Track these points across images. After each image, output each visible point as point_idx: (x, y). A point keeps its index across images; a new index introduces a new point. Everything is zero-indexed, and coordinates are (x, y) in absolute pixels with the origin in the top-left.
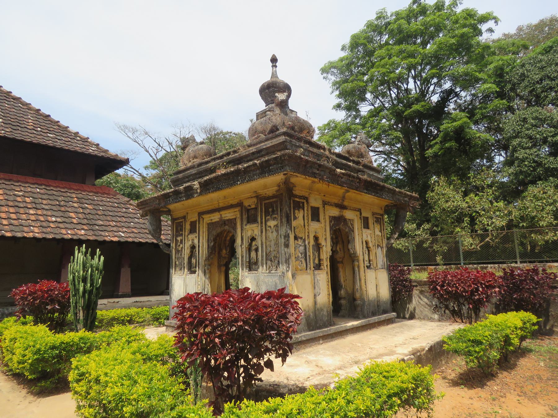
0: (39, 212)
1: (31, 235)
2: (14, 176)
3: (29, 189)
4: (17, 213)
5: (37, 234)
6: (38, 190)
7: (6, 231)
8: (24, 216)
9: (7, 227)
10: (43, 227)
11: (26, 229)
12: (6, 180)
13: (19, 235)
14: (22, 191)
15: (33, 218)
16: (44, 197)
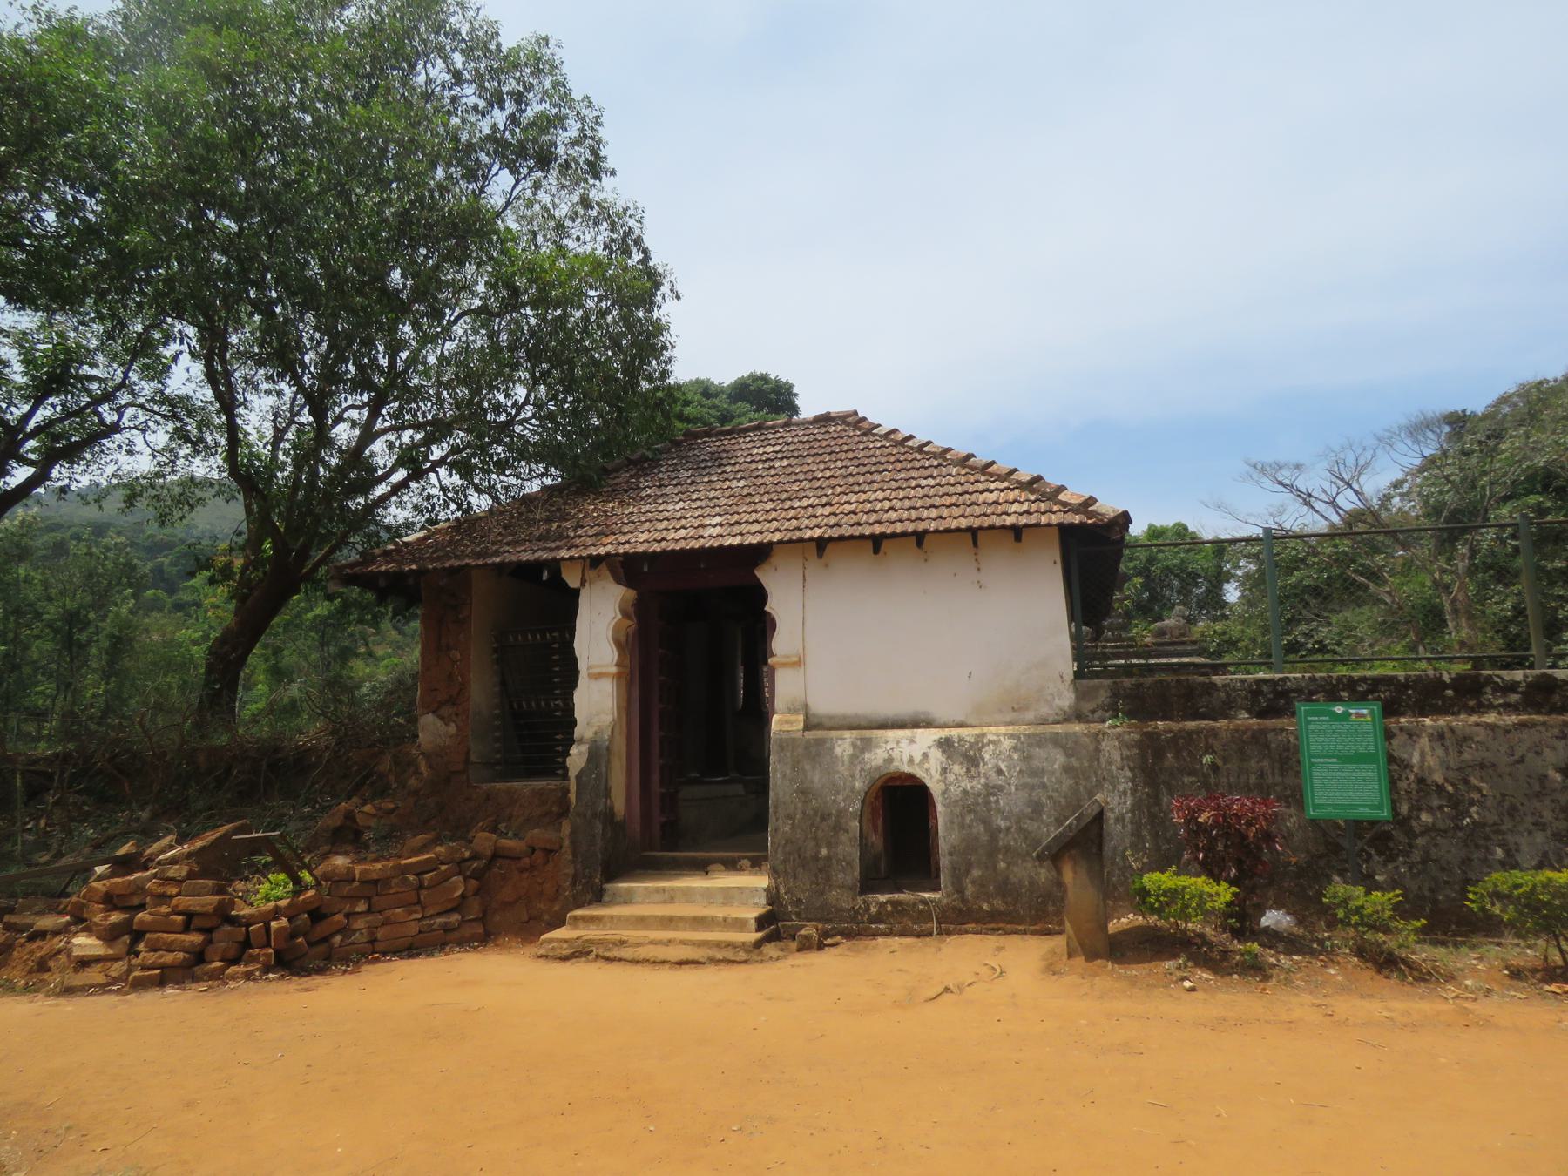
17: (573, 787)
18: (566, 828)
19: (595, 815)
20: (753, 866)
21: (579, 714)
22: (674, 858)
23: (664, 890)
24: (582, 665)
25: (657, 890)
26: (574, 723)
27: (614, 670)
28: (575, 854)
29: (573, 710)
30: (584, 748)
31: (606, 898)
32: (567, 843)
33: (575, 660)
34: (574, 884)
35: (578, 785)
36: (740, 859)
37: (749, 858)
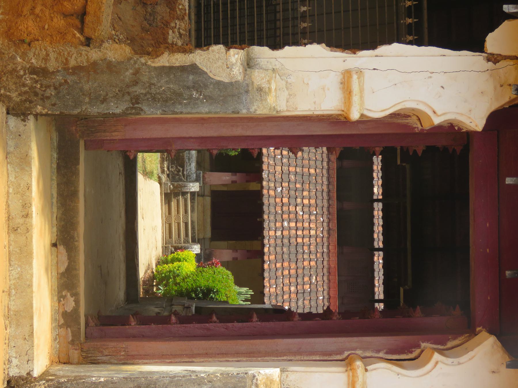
0: (293, 296)
1: (266, 284)
2: (335, 278)
3: (320, 289)
4: (290, 276)
5: (268, 290)
6: (321, 298)
7: (269, 265)
8: (287, 281)
9: (274, 266)
10: (276, 296)
11: (273, 281)
12: (329, 269)
13: (266, 275)
14: (317, 282)
15: (286, 289)
16: (313, 303)
17: (179, 59)
18: (115, 52)
19: (136, 100)
20: (65, 314)
21: (288, 50)
22: (74, 194)
23: (28, 216)
24: (364, 58)
25: (26, 205)
26: (275, 46)
27: (355, 116)
28: (78, 69)
29: (296, 43)
30: (237, 73)
31: (13, 121)
32: (94, 54)
33: (373, 47)
34: (33, 71)
35: (183, 69)
36: (75, 295)
37: (76, 310)
